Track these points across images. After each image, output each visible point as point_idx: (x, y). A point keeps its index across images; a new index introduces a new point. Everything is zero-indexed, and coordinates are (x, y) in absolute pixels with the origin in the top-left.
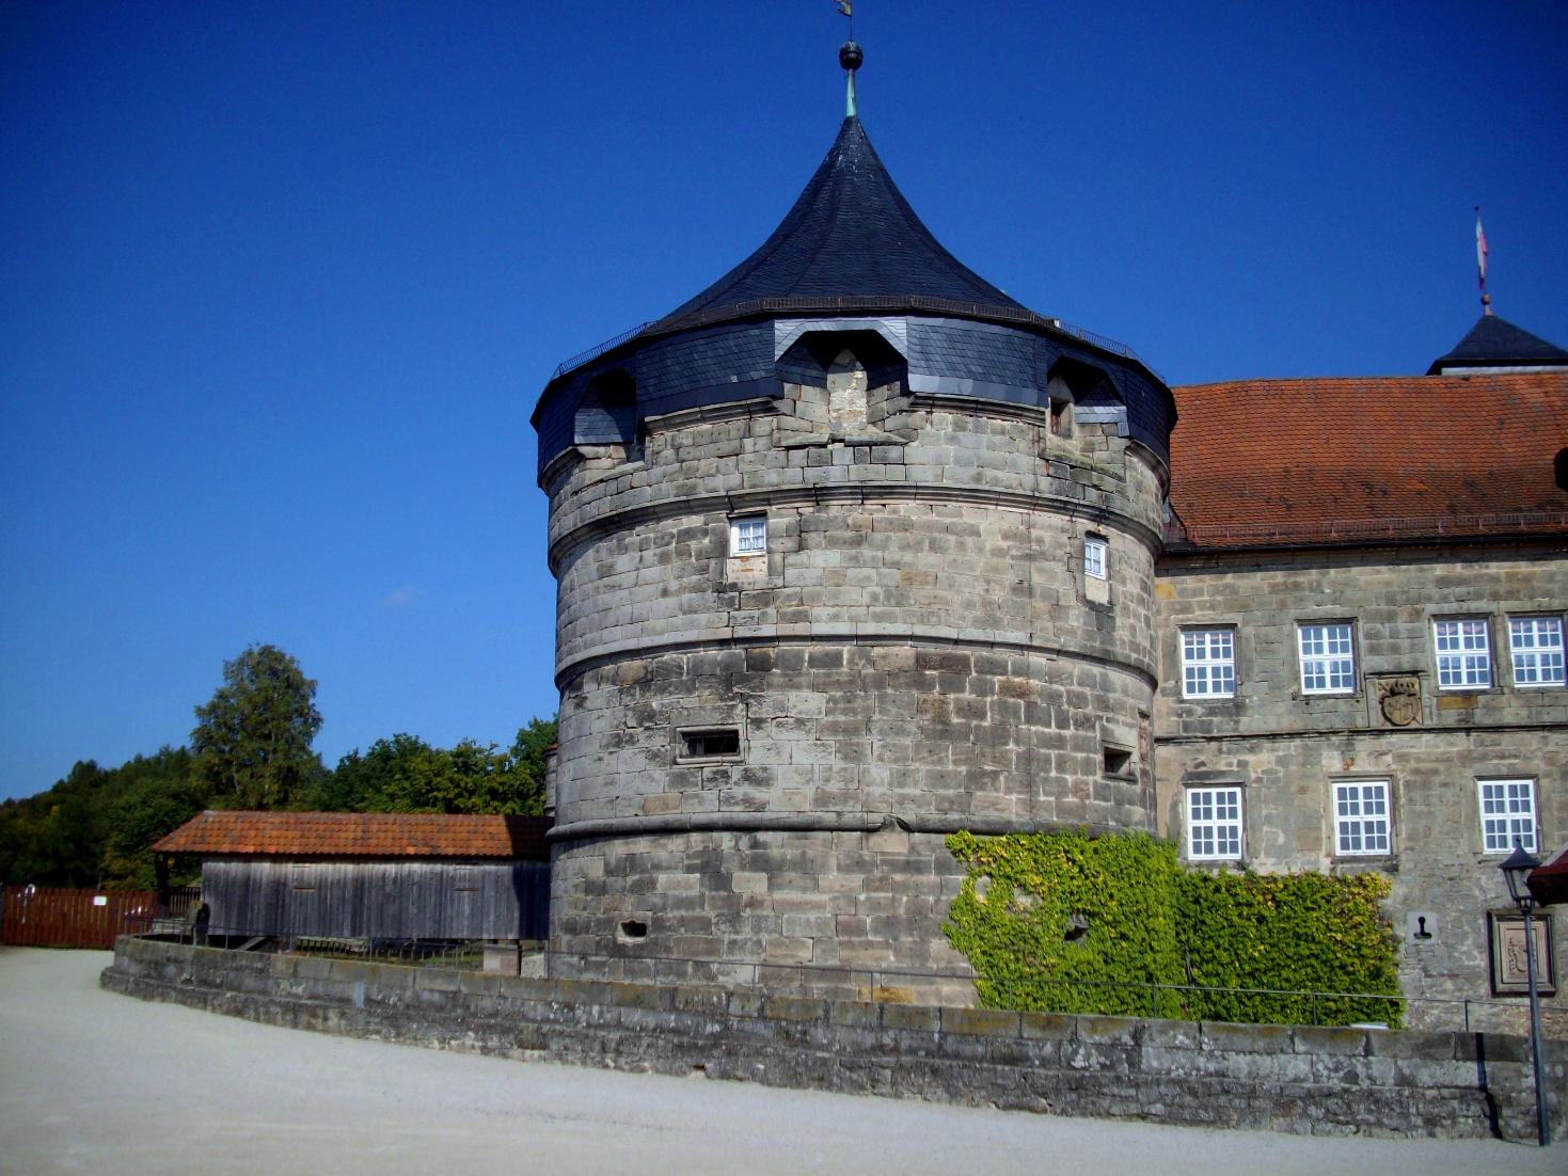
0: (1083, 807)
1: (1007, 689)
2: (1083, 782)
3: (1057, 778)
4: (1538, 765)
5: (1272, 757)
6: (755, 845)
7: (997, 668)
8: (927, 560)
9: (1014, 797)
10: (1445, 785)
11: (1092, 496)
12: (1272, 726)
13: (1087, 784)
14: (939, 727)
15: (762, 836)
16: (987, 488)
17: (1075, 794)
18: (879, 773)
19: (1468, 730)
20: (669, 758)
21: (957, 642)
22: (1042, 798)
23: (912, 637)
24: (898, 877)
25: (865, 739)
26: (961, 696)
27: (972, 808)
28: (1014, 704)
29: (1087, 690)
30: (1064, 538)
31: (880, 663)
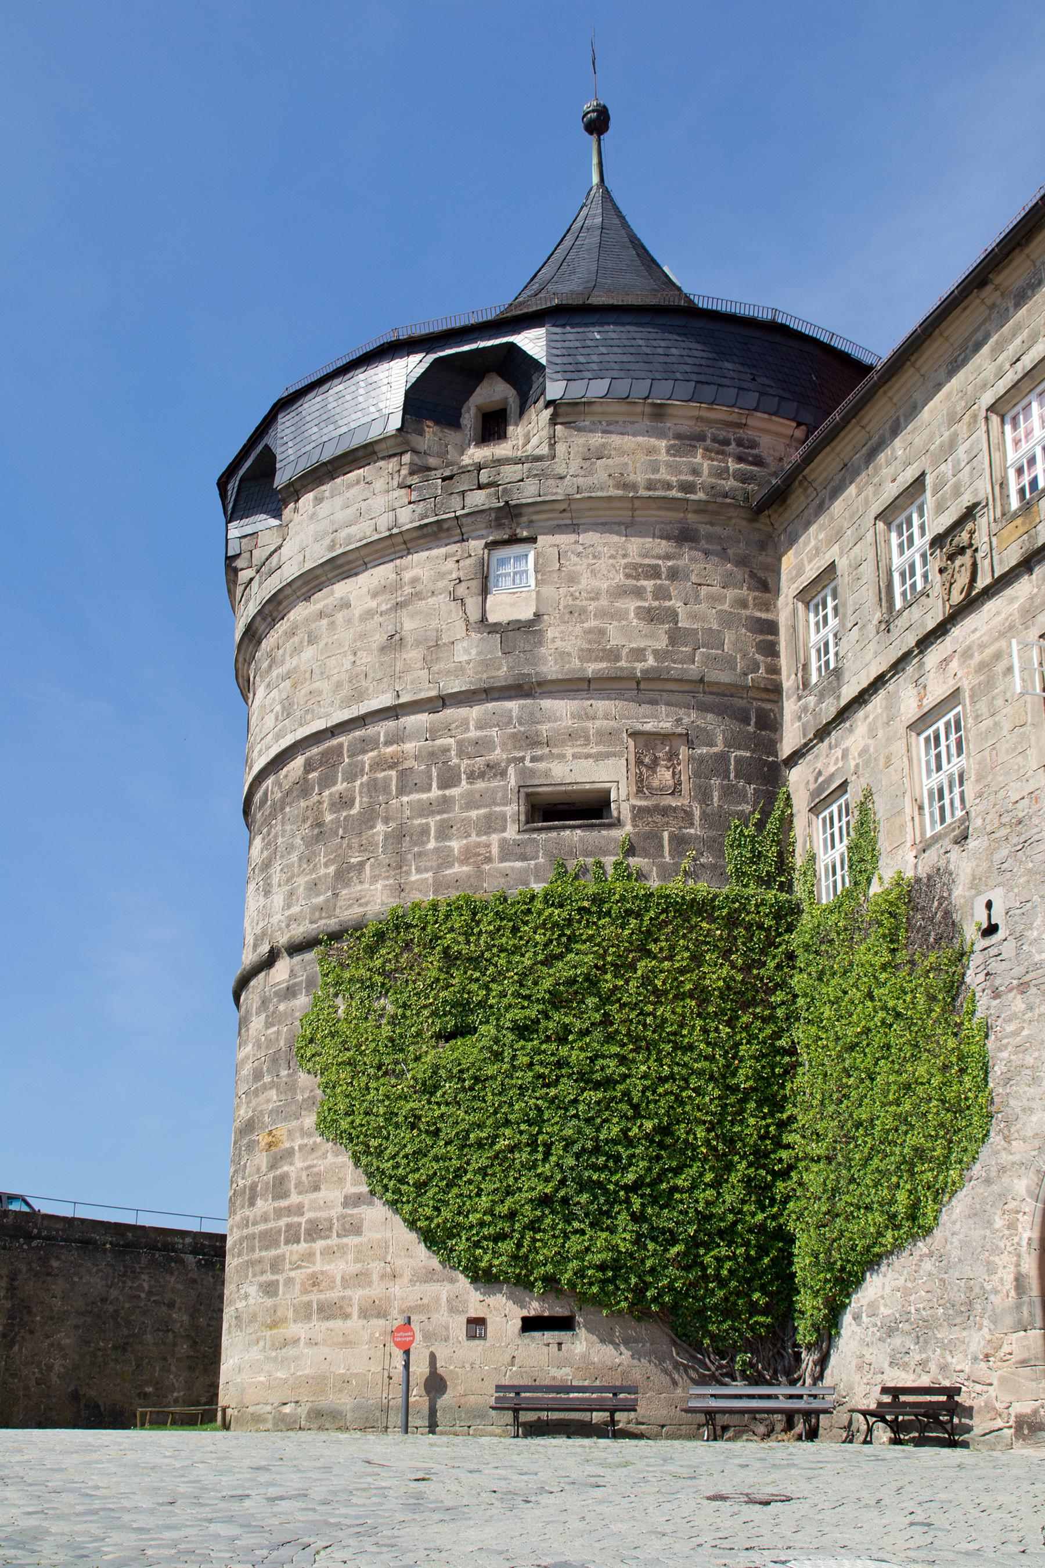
0: (480, 874)
1: (379, 764)
2: (478, 845)
3: (437, 850)
8: (309, 653)
9: (379, 885)
11: (479, 499)
13: (488, 846)
14: (316, 831)
16: (341, 551)
17: (462, 862)
18: (278, 899)
21: (333, 731)
22: (414, 877)
24: (282, 1007)
26: (334, 789)
27: (338, 911)
28: (385, 778)
29: (494, 732)
30: (450, 564)
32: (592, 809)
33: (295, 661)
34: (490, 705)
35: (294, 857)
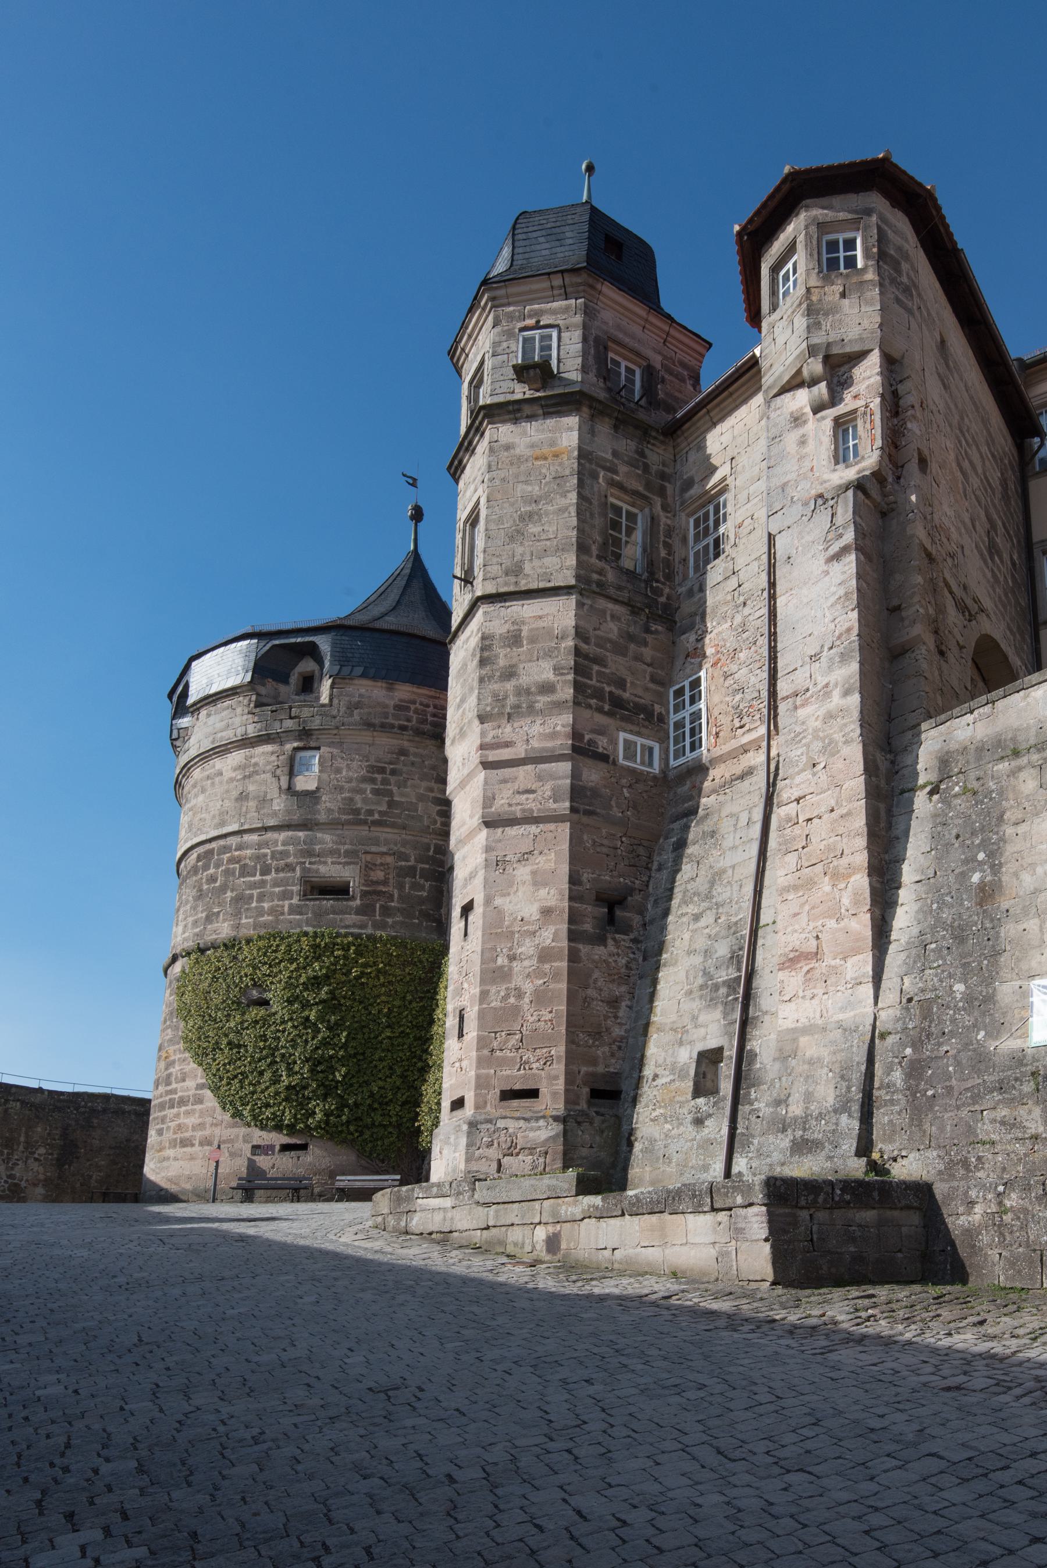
1: (232, 860)
2: (278, 906)
7: (226, 849)
9: (226, 925)
13: (283, 906)
17: (269, 915)
22: (244, 921)
29: (291, 848)
32: (340, 891)
34: (290, 833)
35: (188, 907)
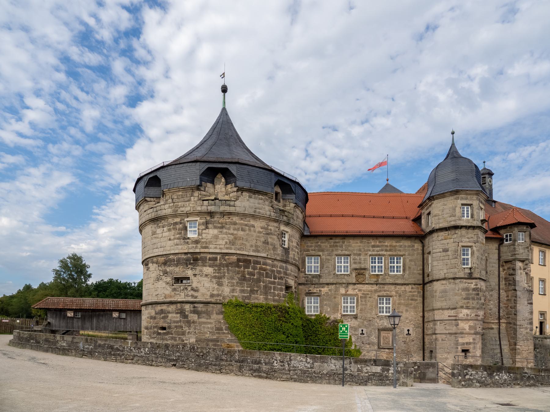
1: (261, 269)
4: (394, 293)
5: (328, 289)
6: (194, 307)
8: (241, 233)
9: (262, 297)
10: (370, 297)
12: (328, 281)
15: (196, 305)
19: (377, 284)
20: (171, 284)
21: (248, 255)
23: (236, 254)
25: (223, 280)
29: (282, 270)
31: (227, 260)
33: (235, 232)
